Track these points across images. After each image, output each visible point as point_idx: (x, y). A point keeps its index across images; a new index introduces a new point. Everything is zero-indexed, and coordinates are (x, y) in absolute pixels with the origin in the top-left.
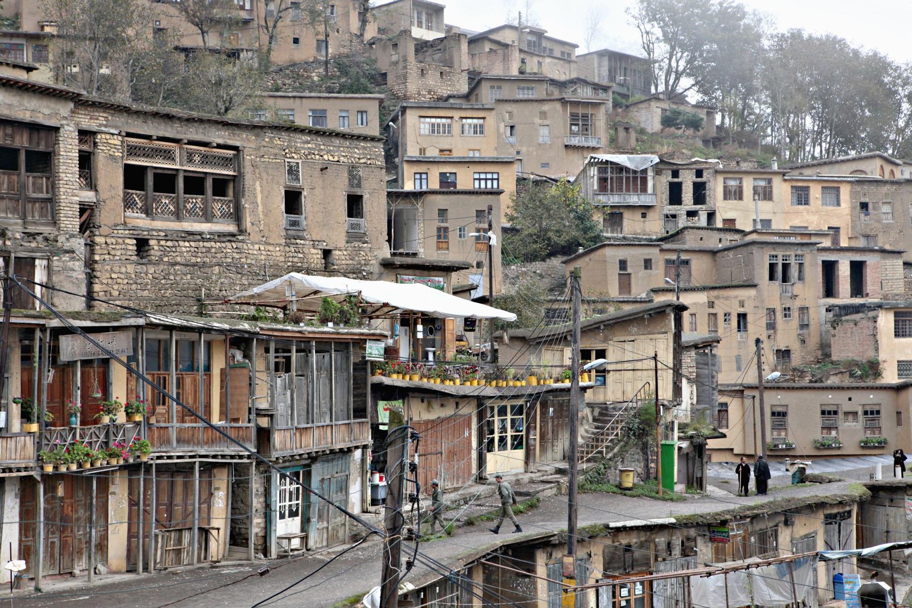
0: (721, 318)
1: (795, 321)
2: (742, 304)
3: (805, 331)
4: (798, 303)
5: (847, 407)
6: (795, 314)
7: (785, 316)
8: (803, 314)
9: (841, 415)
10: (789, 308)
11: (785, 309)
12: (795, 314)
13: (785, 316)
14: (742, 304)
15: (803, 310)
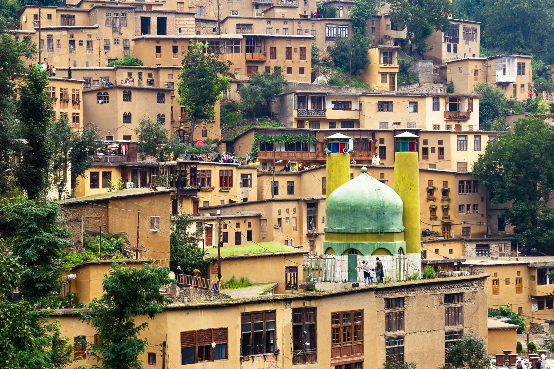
0: (77, 43)
1: (121, 46)
2: (90, 36)
3: (128, 52)
4: (124, 36)
5: (94, 78)
6: (121, 42)
7: (115, 43)
8: (126, 43)
9: (92, 81)
10: (118, 40)
11: (115, 39)
12: (121, 42)
13: (115, 43)
14: (90, 36)
15: (126, 40)
